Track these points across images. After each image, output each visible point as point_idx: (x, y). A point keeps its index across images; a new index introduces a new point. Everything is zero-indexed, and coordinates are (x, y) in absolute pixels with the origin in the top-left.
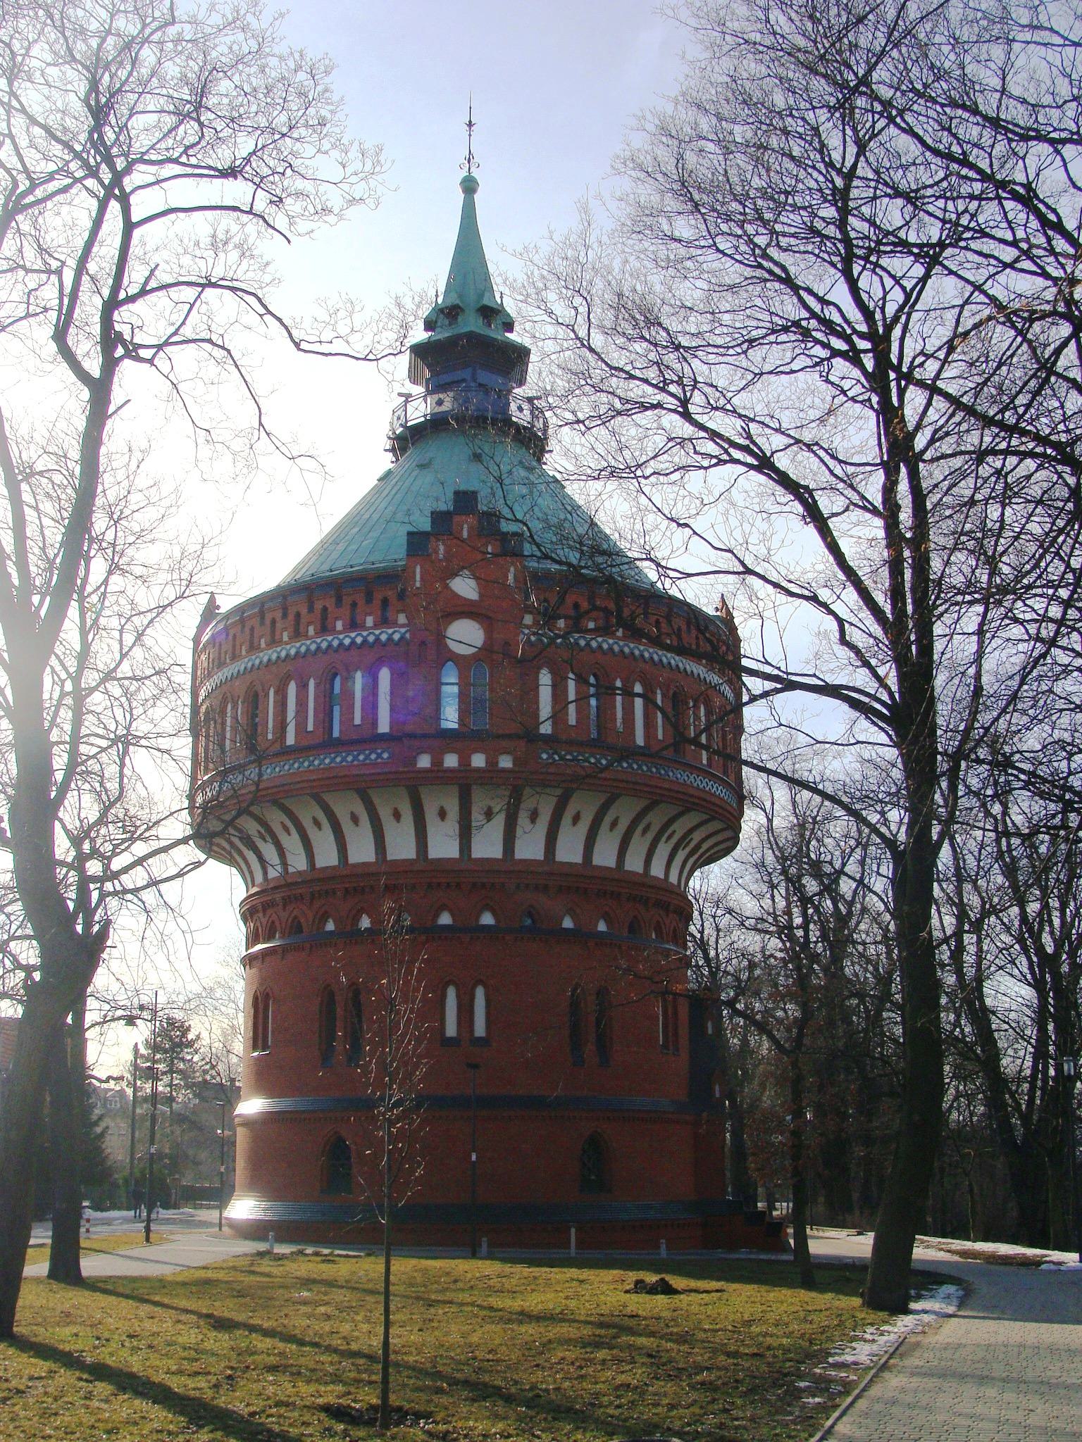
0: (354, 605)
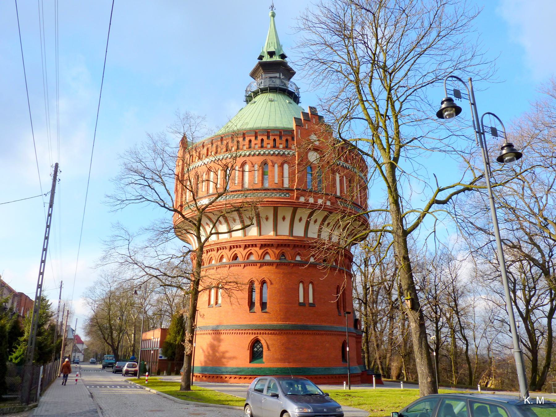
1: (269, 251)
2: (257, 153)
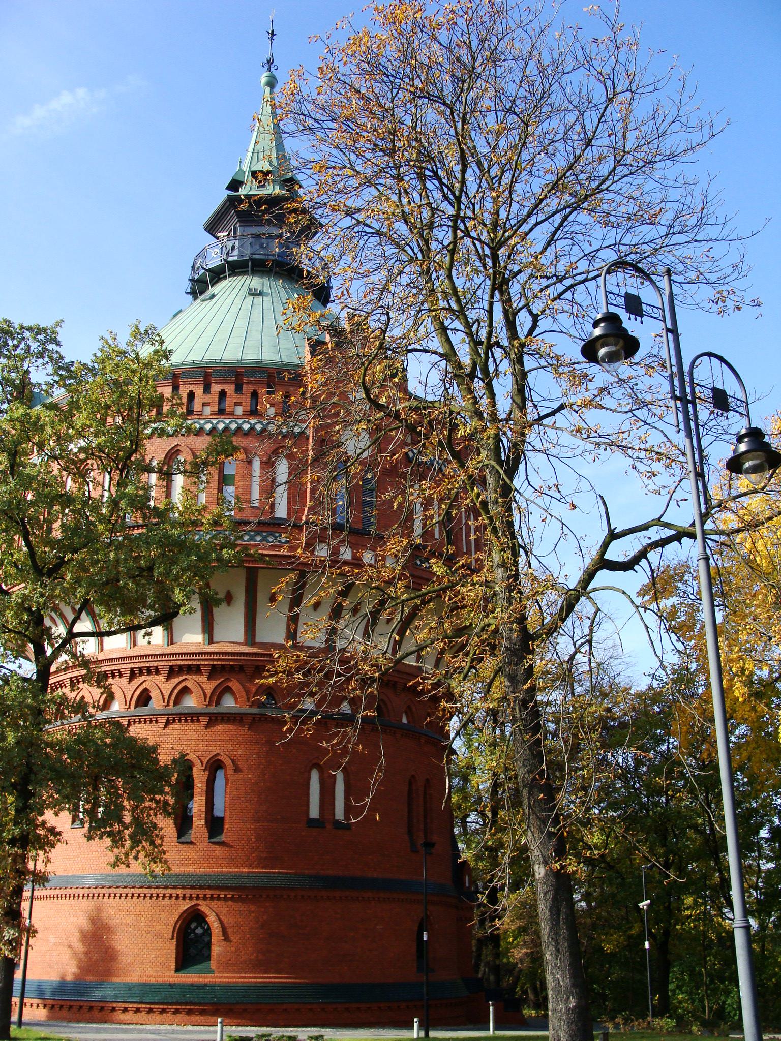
1: (234, 684)
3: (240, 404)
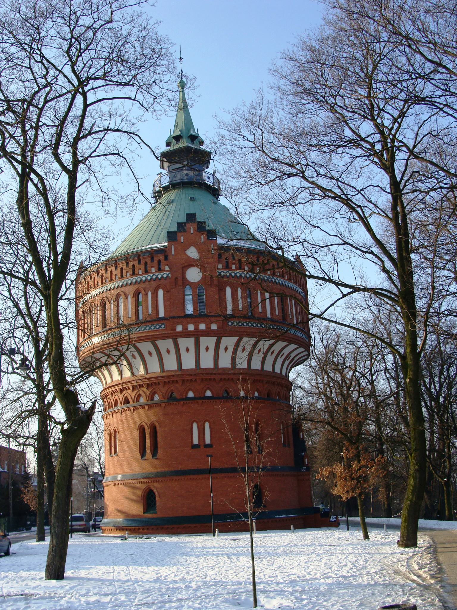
0: (146, 264)
2: (130, 282)
3: (140, 269)
